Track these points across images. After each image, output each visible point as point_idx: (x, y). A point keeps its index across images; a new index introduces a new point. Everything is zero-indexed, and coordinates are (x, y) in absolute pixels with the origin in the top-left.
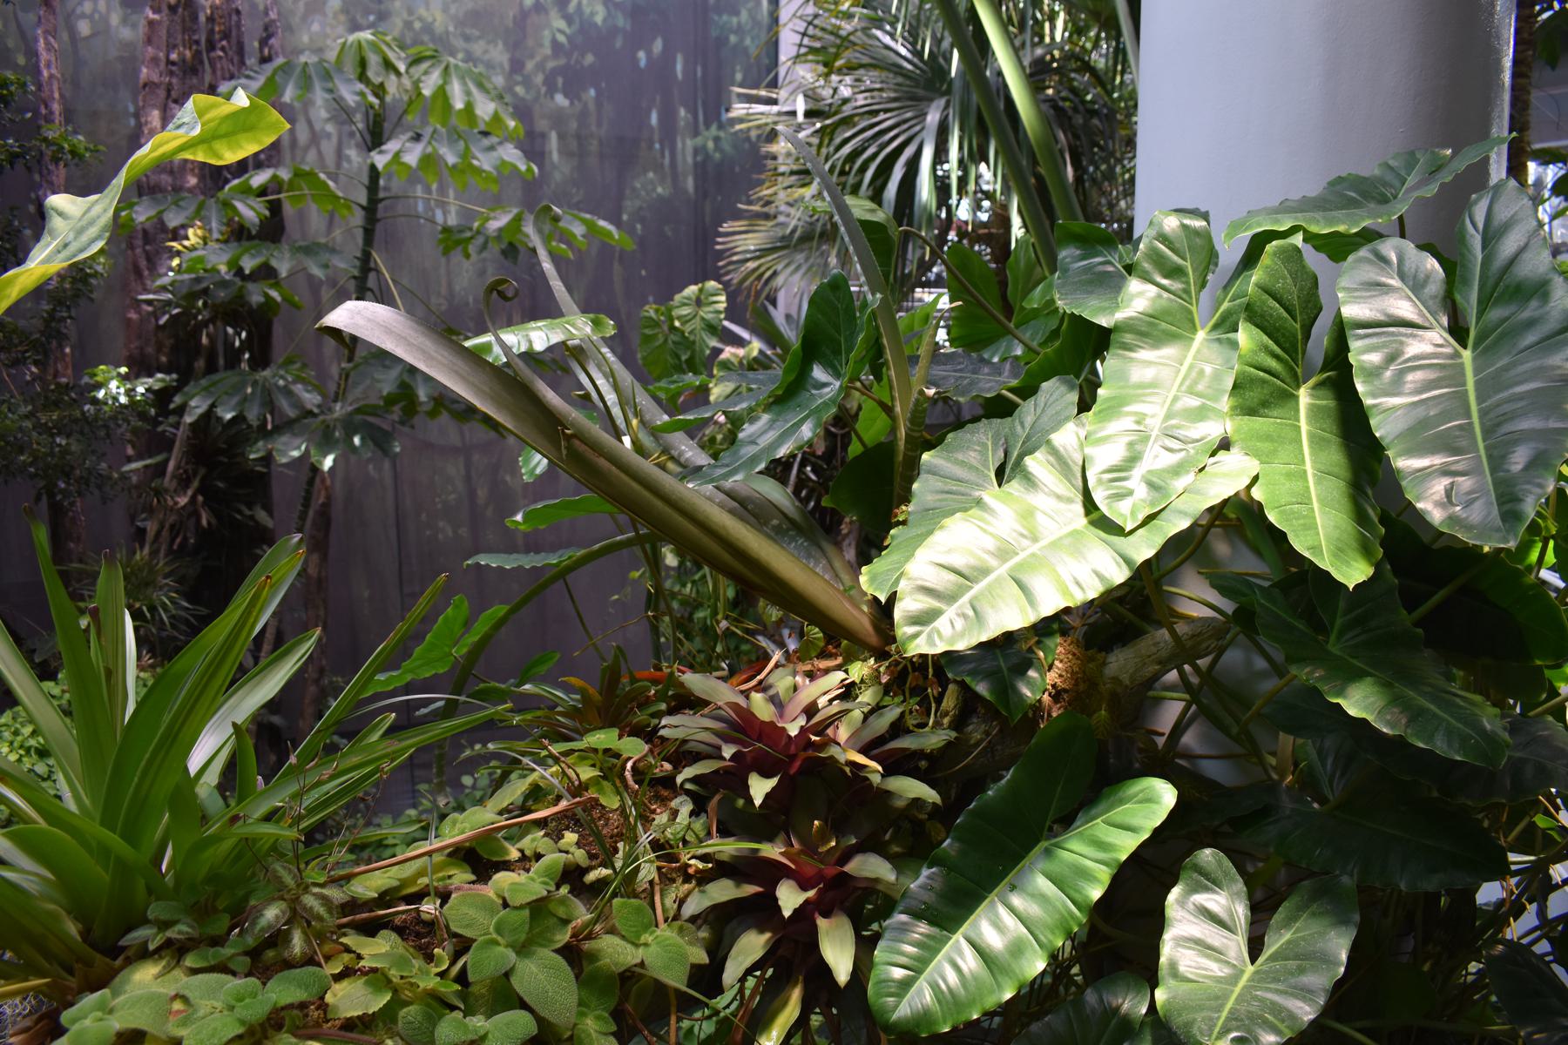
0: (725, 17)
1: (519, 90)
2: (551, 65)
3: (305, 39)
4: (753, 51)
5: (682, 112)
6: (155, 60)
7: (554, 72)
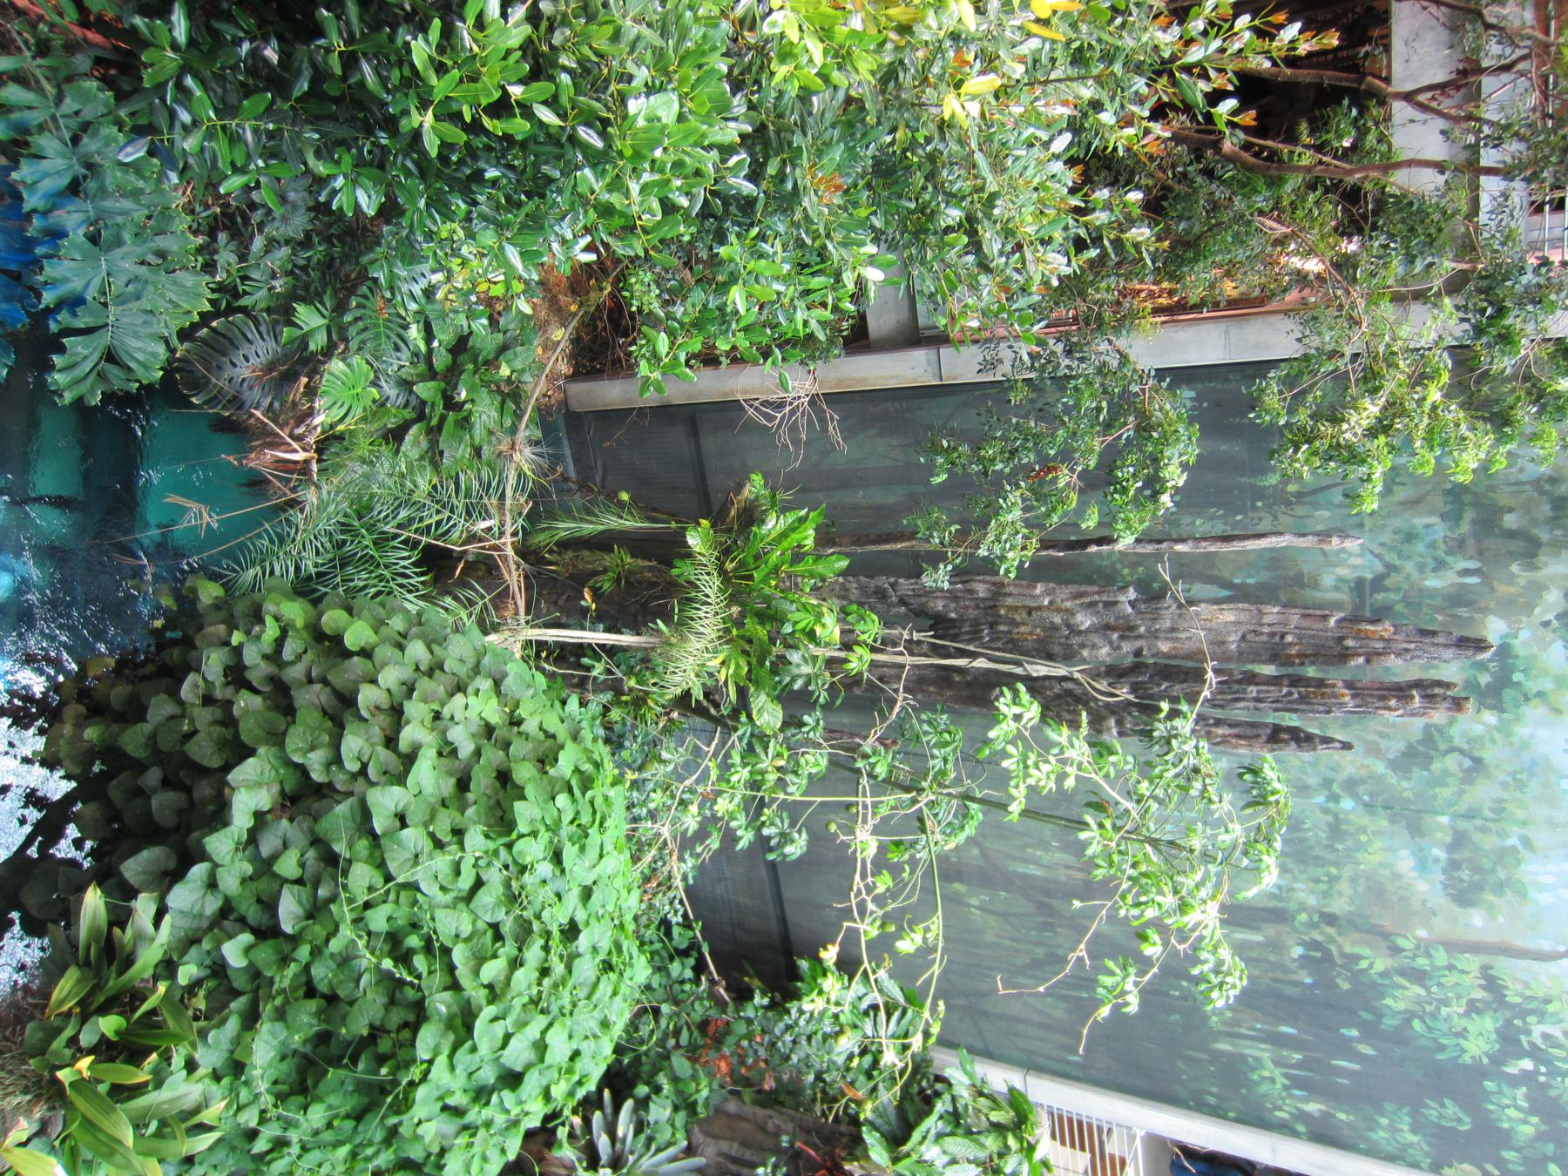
0: (1407, 1119)
1: (1303, 917)
2: (1333, 948)
4: (1373, 1136)
5: (1298, 1056)
7: (1327, 952)
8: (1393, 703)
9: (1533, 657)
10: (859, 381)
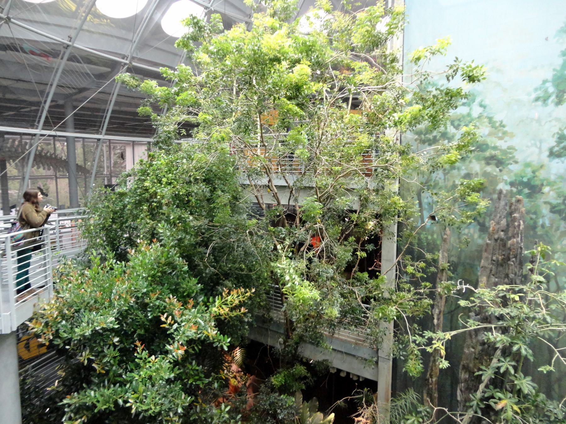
3: (559, 247)
6: (487, 258)
8: (516, 224)
9: (516, 175)
10: (387, 392)
